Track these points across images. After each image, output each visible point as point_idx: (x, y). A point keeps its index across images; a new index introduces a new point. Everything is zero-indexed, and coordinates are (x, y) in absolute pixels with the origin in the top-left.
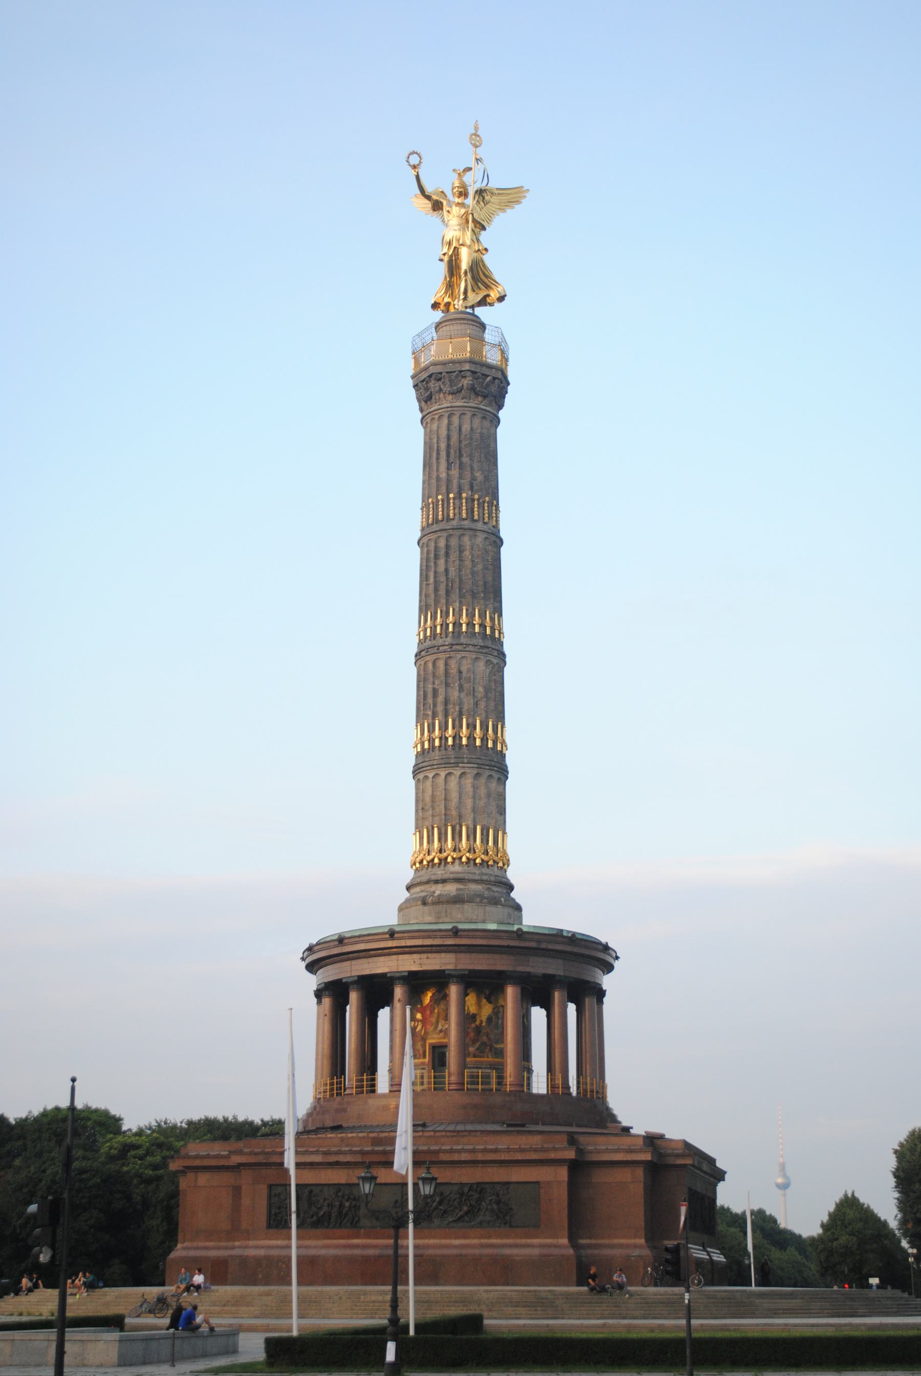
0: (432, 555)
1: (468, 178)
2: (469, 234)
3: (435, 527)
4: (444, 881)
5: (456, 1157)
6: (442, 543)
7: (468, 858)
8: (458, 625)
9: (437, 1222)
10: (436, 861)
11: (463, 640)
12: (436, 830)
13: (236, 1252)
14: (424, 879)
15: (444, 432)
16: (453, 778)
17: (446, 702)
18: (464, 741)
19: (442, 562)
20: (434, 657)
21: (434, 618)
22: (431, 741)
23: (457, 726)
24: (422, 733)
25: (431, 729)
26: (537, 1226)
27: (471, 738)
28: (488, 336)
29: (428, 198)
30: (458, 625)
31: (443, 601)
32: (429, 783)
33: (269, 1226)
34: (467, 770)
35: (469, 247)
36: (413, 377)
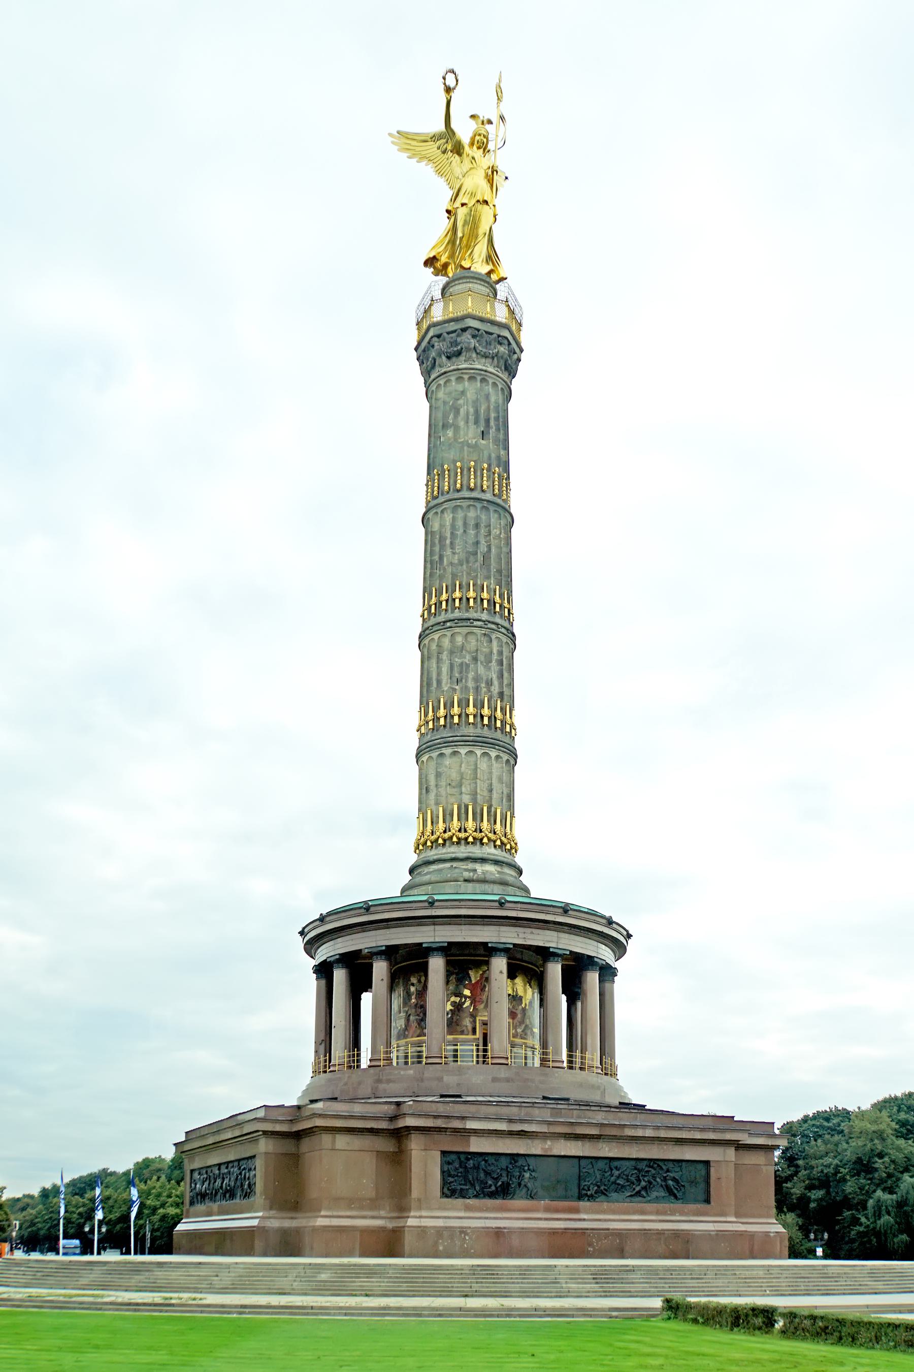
0: (460, 523)
3: (466, 494)
4: (483, 860)
5: (640, 1133)
7: (502, 843)
9: (614, 1195)
10: (471, 839)
11: (498, 620)
12: (470, 808)
14: (461, 855)
15: (471, 395)
16: (486, 759)
18: (499, 724)
19: (472, 532)
20: (465, 630)
34: (502, 754)
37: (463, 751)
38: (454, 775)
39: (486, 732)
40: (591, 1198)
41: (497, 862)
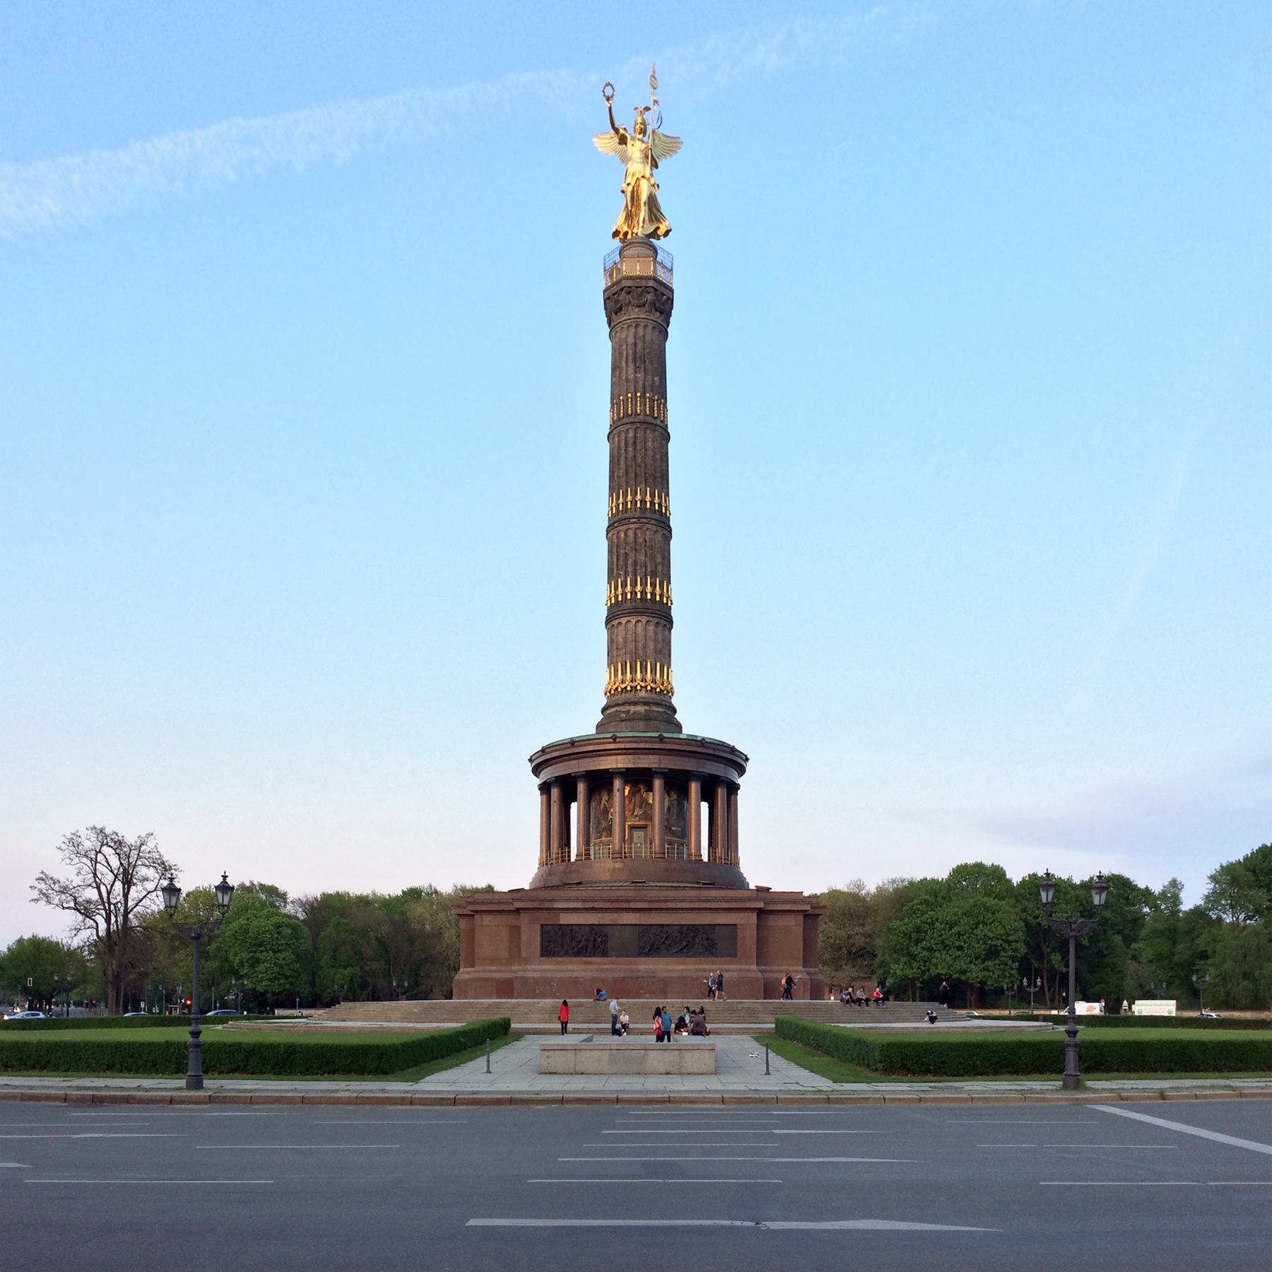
1: (647, 115)
2: (648, 168)
3: (626, 420)
4: (635, 703)
6: (631, 434)
8: (643, 502)
11: (648, 515)
13: (520, 974)
15: (631, 340)
17: (635, 563)
21: (625, 496)
22: (624, 594)
23: (644, 584)
24: (616, 589)
25: (624, 585)
26: (735, 956)
27: (653, 594)
28: (659, 258)
29: (616, 130)
30: (643, 502)
31: (632, 482)
32: (622, 627)
33: (542, 955)
35: (648, 180)
36: (605, 291)
37: (624, 620)
38: (620, 640)
39: (639, 604)
40: (647, 955)
41: (645, 703)
